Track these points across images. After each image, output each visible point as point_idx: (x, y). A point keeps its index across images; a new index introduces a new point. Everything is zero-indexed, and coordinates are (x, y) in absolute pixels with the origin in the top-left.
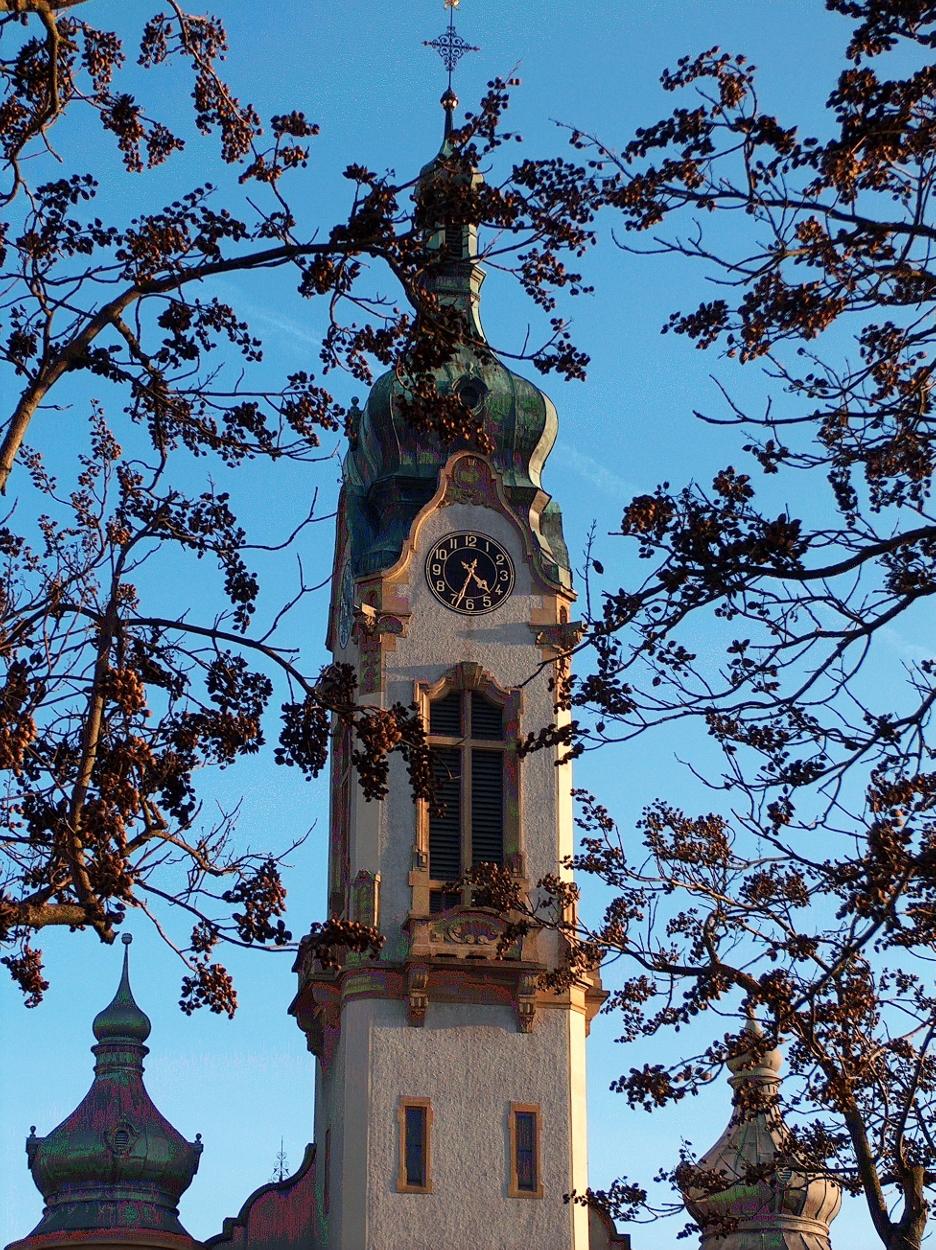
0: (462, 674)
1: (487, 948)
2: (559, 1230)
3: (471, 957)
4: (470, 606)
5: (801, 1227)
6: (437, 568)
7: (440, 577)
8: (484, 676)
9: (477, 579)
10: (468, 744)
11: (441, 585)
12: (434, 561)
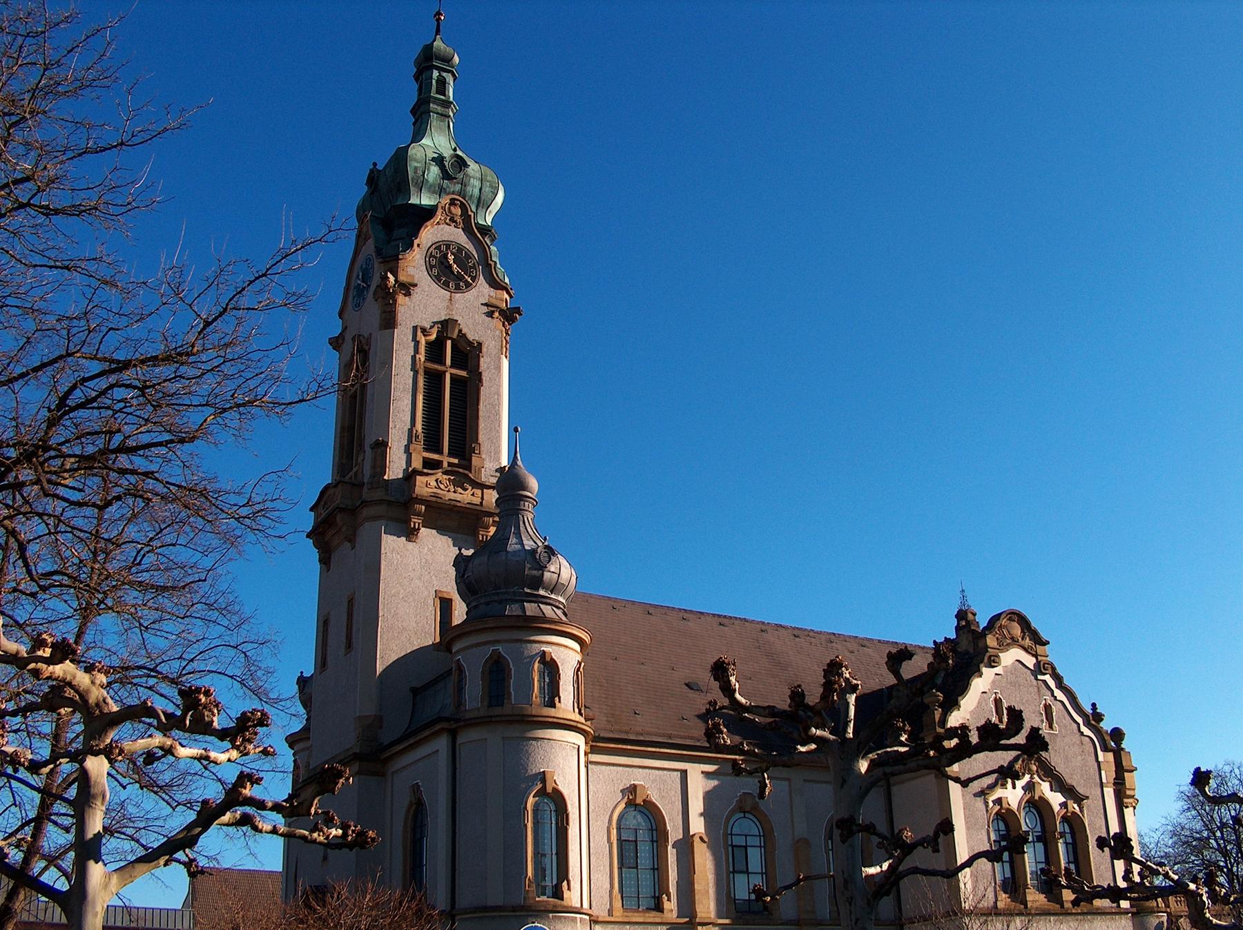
0: (446, 325)
4: (452, 287)
6: (433, 260)
7: (434, 266)
12: (431, 256)
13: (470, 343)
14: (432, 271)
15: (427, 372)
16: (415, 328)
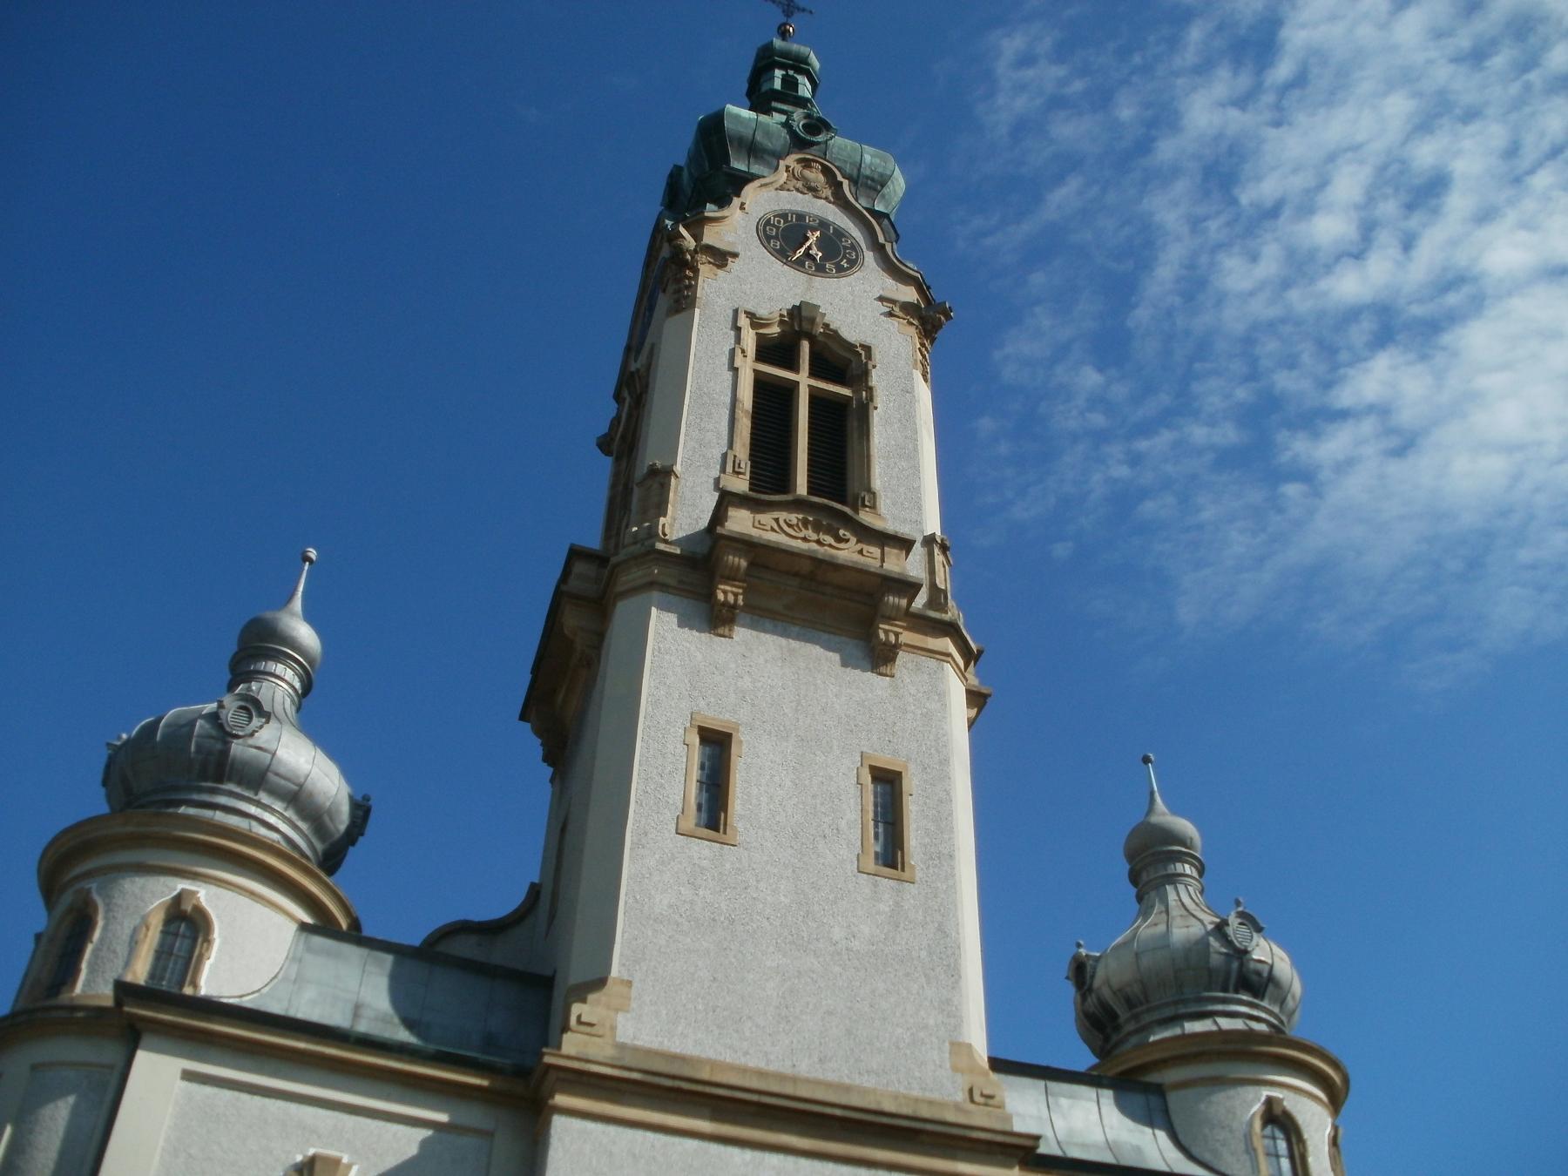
0: (799, 321)
2: (941, 929)
10: (804, 380)
13: (850, 347)
16: (736, 312)
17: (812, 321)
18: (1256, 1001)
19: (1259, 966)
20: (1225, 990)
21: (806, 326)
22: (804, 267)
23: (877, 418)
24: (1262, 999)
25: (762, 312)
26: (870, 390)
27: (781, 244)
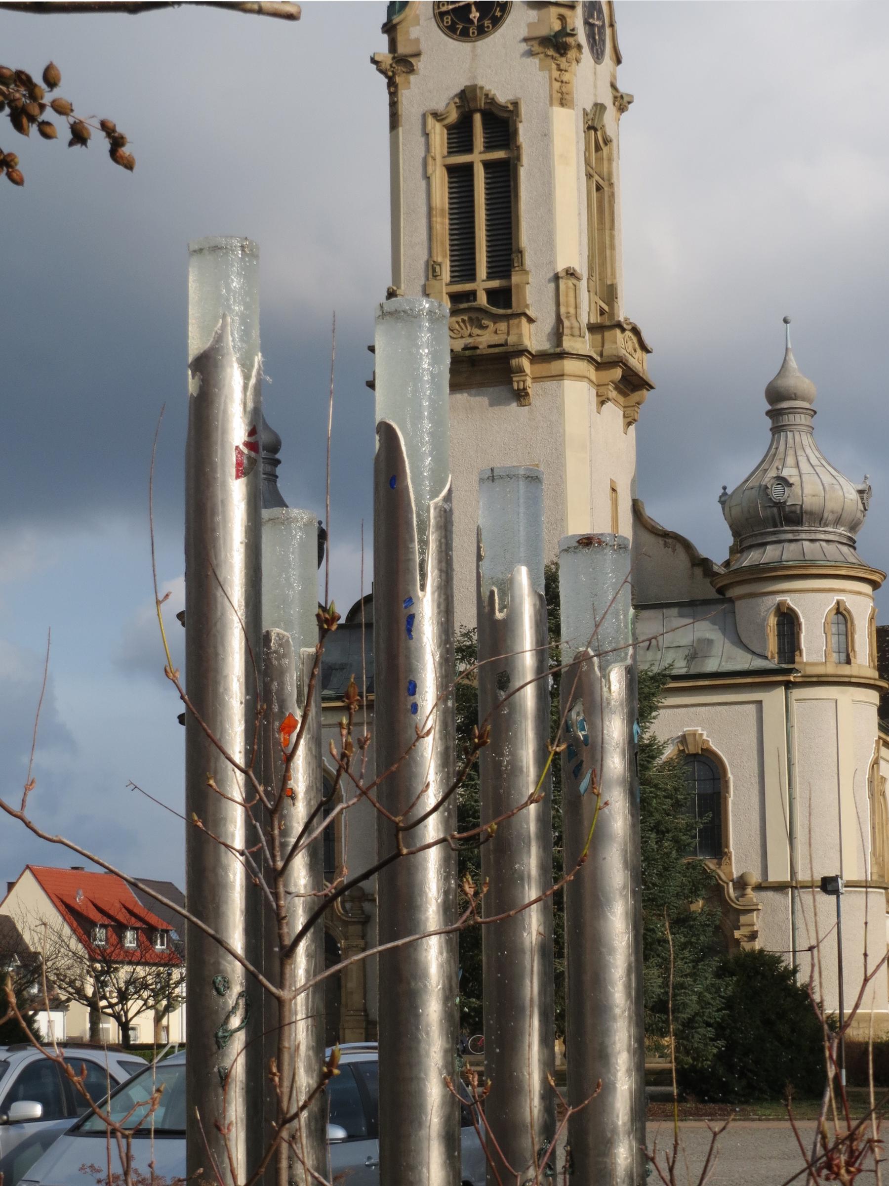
1: (480, 339)
3: (466, 348)
4: (473, 33)
5: (803, 536)
8: (487, 95)
9: (473, 9)
11: (448, 19)
13: (504, 108)
14: (443, 21)
15: (451, 170)
16: (424, 116)
17: (475, 98)
18: (795, 528)
19: (793, 508)
20: (775, 526)
21: (472, 105)
22: (469, 37)
23: (523, 173)
24: (802, 526)
25: (440, 107)
26: (518, 148)
27: (452, 19)
